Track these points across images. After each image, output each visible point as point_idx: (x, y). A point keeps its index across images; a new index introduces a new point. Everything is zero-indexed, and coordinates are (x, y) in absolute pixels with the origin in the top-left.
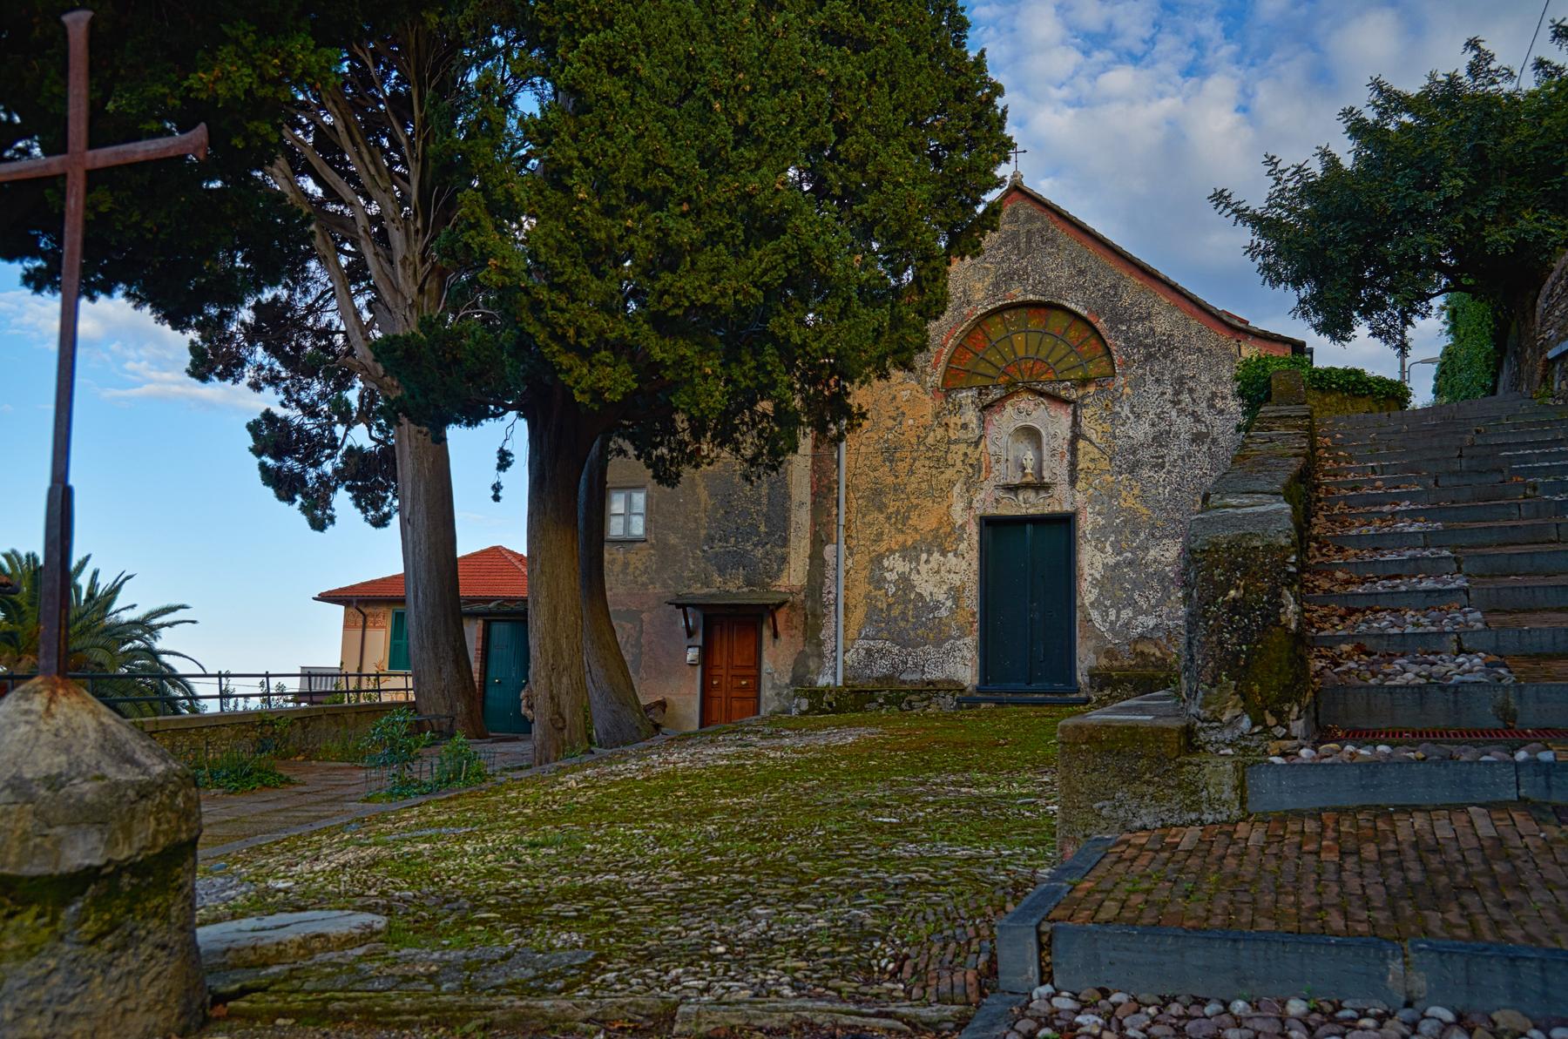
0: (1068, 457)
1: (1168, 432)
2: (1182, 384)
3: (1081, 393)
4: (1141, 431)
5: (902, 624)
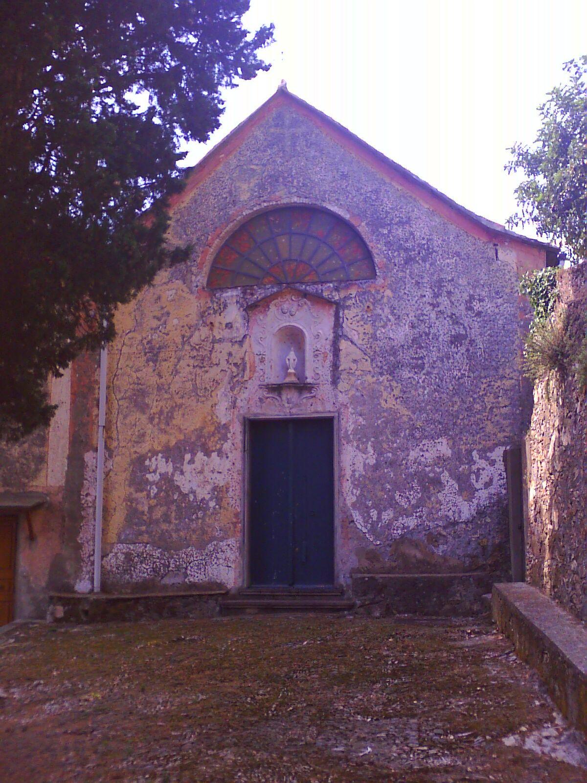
0: (330, 357)
1: (427, 334)
2: (440, 287)
3: (343, 294)
4: (401, 334)
5: (164, 526)
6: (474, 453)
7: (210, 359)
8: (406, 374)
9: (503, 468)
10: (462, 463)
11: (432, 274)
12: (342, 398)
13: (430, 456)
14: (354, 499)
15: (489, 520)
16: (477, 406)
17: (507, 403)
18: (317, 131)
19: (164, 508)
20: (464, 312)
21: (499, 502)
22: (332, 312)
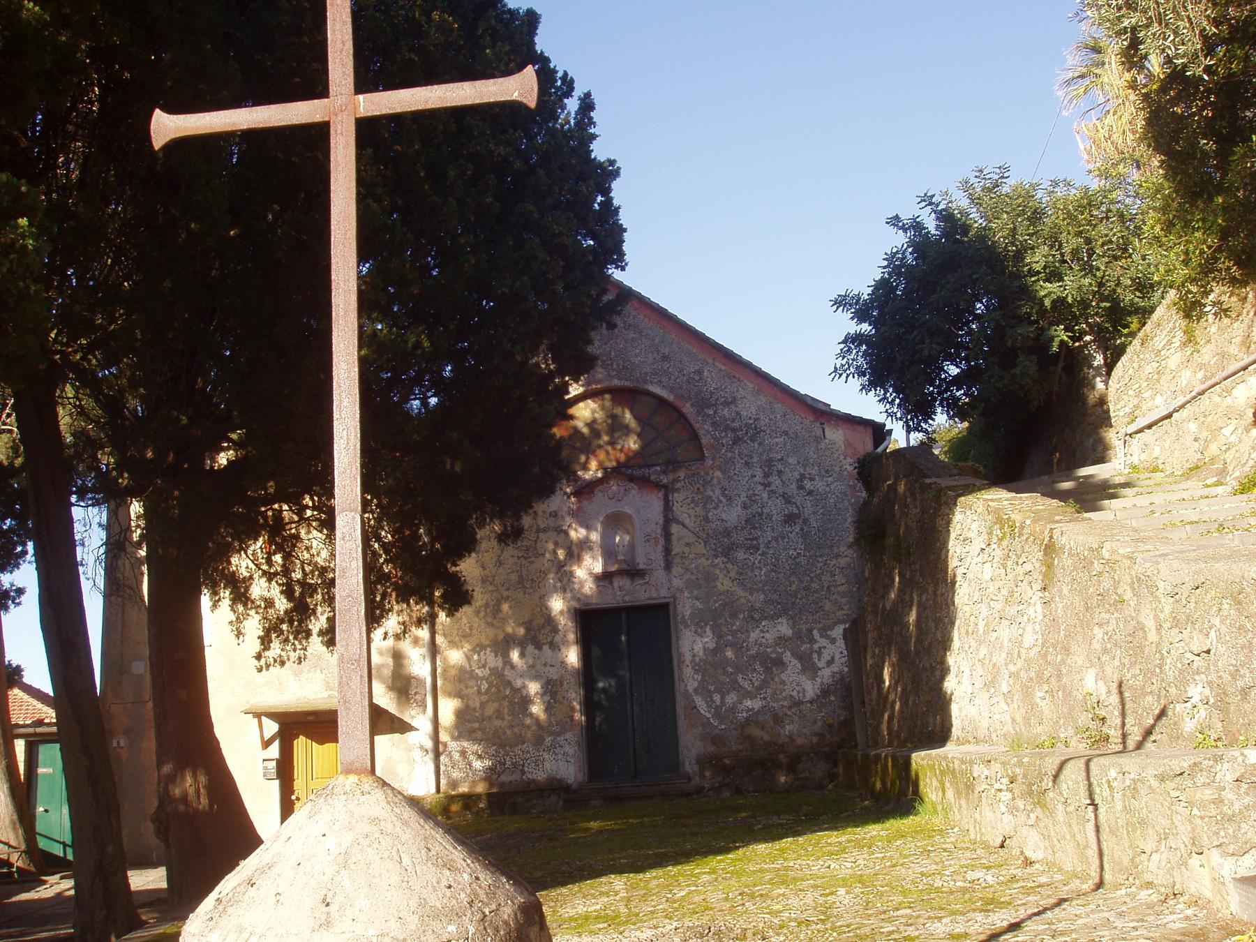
0: (662, 542)
1: (761, 515)
2: (770, 466)
3: (671, 477)
4: (733, 515)
5: (498, 723)
6: (815, 632)
7: (535, 549)
8: (741, 555)
9: (843, 646)
10: (803, 642)
11: (761, 454)
12: (676, 582)
13: (770, 637)
14: (696, 684)
15: (833, 698)
16: (815, 586)
17: (844, 581)
18: (635, 313)
19: (496, 705)
20: (796, 492)
21: (842, 679)
22: (661, 495)
